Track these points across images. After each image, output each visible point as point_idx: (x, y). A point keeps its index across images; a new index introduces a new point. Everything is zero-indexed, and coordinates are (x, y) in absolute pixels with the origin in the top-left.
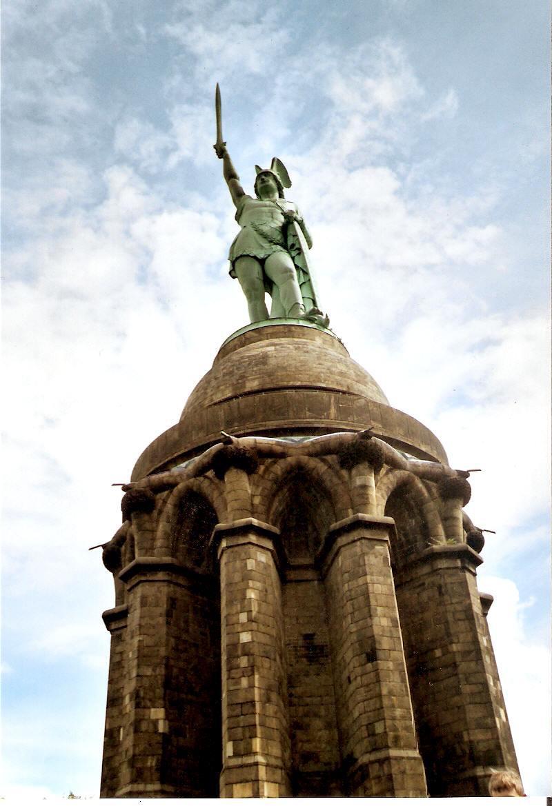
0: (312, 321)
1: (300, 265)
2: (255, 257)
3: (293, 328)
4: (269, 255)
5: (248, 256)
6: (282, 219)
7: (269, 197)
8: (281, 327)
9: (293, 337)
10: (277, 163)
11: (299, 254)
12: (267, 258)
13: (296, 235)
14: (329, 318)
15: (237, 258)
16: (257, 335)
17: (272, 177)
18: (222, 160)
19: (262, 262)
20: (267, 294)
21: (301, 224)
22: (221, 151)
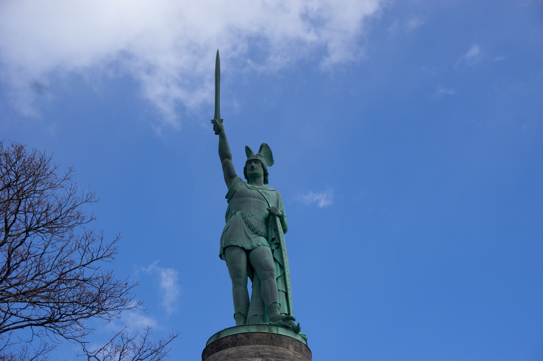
0: (287, 327)
1: (278, 259)
2: (243, 248)
4: (255, 248)
5: (238, 246)
6: (267, 212)
7: (256, 184)
9: (273, 345)
10: (264, 147)
11: (278, 248)
12: (253, 249)
13: (276, 230)
14: (301, 326)
15: (228, 247)
16: (246, 339)
17: (260, 165)
18: (218, 136)
19: (248, 252)
20: (249, 279)
21: (281, 218)
22: (218, 130)
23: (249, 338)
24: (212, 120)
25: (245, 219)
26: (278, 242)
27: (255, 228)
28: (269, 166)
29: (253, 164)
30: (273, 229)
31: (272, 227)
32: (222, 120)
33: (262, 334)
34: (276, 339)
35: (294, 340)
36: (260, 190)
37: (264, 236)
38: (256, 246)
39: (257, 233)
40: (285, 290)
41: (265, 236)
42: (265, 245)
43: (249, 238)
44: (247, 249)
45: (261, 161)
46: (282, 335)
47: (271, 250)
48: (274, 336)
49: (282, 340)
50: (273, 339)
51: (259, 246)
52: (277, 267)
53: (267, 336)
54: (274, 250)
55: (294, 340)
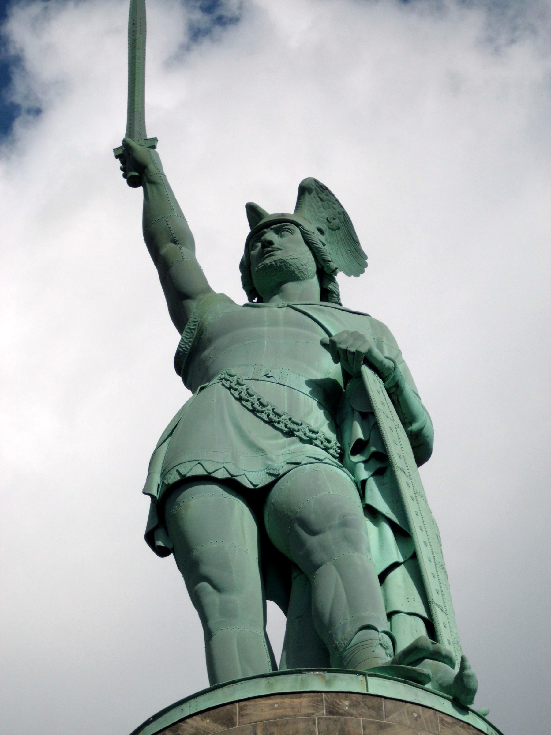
3: (346, 704)
8: (304, 700)
23: (233, 724)
24: (115, 150)
25: (236, 390)
26: (381, 450)
27: (279, 411)
28: (348, 274)
29: (270, 235)
30: (357, 414)
31: (353, 410)
32: (155, 140)
33: (287, 700)
34: (355, 712)
35: (448, 719)
36: (298, 307)
37: (322, 443)
38: (287, 467)
39: (290, 433)
40: (423, 612)
41: (326, 443)
42: (320, 461)
43: (260, 450)
44: (251, 486)
45: (298, 225)
46: (385, 698)
47: (356, 483)
48: (347, 703)
49: (387, 717)
50: (342, 715)
51: (298, 464)
52: (381, 535)
53: (313, 706)
54: (364, 482)
55: (448, 719)
